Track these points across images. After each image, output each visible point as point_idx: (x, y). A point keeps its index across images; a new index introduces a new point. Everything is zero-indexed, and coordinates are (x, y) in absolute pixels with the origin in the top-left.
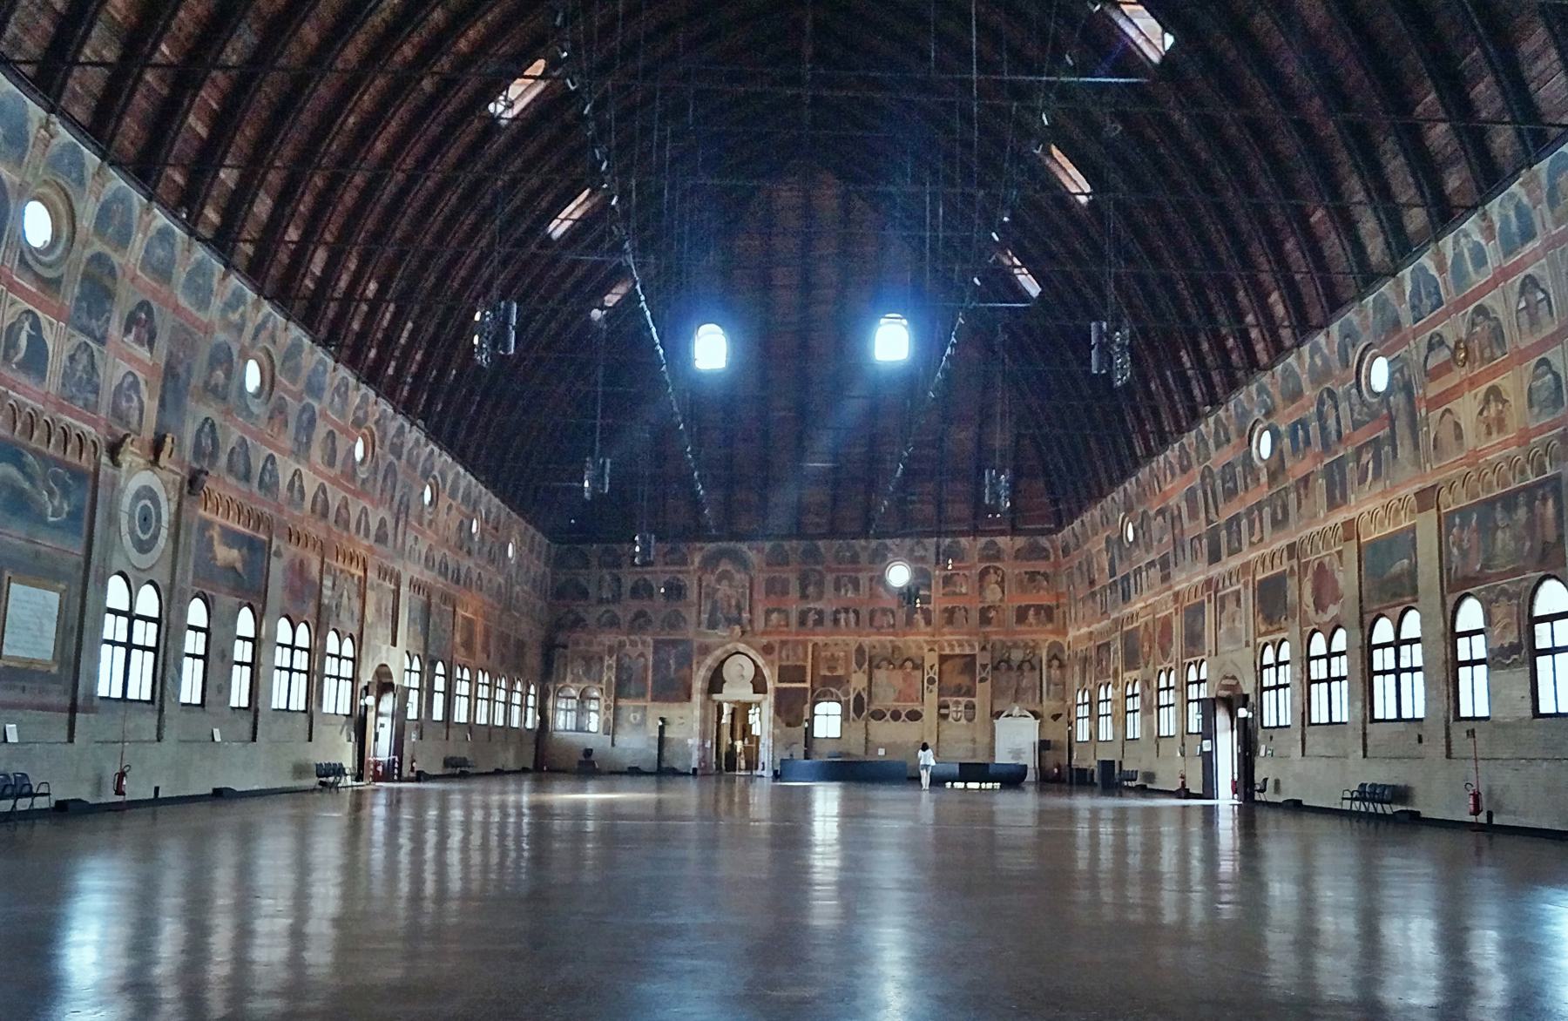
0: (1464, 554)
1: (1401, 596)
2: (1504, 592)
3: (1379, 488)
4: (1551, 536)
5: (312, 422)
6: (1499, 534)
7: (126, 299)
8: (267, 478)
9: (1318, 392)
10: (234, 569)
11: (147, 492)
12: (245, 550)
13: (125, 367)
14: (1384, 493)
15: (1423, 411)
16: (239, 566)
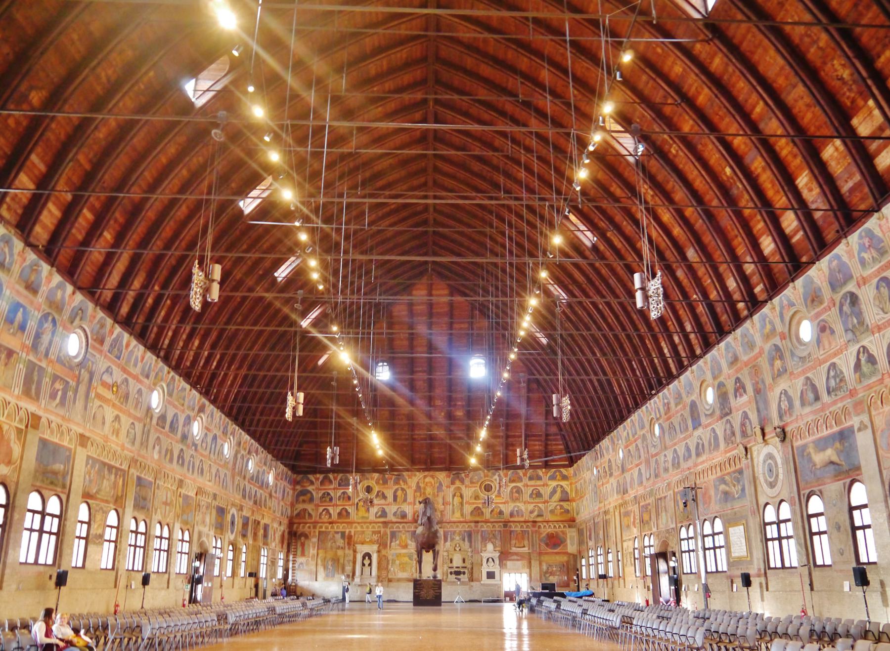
0: (90, 481)
1: (56, 485)
2: (101, 508)
3: (61, 412)
4: (120, 494)
5: (854, 299)
6: (105, 481)
7: (730, 387)
8: (832, 383)
9: (48, 310)
10: (832, 463)
11: (770, 456)
12: (838, 445)
13: (740, 412)
14: (63, 418)
15: (93, 395)
16: (835, 458)
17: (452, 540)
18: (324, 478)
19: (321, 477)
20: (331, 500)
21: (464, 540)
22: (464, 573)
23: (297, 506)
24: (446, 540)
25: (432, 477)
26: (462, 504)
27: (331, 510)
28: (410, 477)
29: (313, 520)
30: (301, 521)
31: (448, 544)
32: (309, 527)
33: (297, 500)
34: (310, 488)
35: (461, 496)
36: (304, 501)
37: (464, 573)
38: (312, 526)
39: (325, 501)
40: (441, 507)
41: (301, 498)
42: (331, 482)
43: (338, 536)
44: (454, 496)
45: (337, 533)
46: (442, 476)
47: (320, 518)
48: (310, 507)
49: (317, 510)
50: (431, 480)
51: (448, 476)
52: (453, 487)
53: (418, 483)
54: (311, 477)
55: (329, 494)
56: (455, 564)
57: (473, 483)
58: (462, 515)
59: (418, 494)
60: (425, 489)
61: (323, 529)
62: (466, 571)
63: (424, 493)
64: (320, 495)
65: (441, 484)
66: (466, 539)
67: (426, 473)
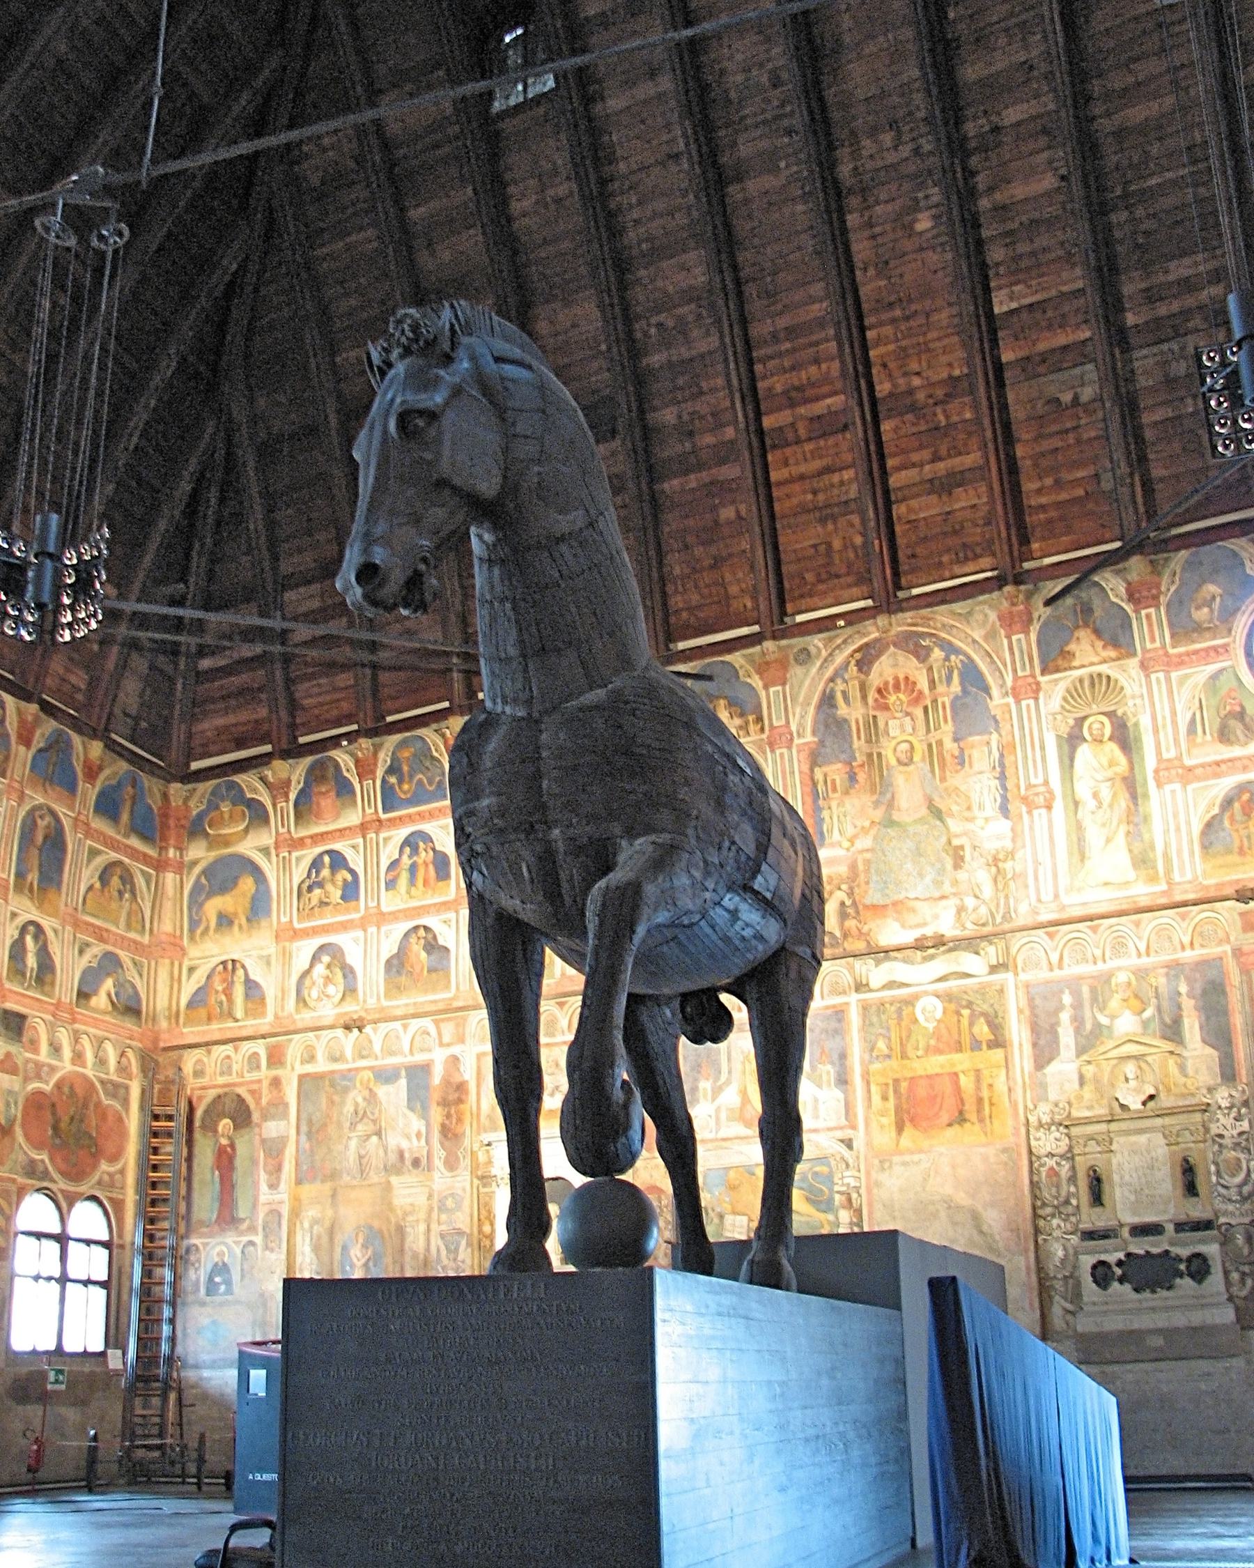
17: (1088, 1040)
18: (316, 775)
19: (296, 772)
20: (350, 891)
21: (1173, 1031)
22: (1199, 1268)
23: (194, 952)
24: (1044, 1053)
25: (915, 646)
26: (1131, 786)
27: (350, 944)
28: (774, 671)
29: (265, 1023)
30: (215, 1029)
31: (1064, 1068)
32: (254, 1058)
33: (194, 924)
34: (248, 847)
35: (1124, 736)
36: (225, 921)
37: (1199, 1268)
38: (260, 1047)
39: (323, 904)
40: (992, 832)
41: (213, 906)
42: (344, 790)
43: (394, 1095)
44: (1073, 740)
45: (386, 1076)
46: (977, 630)
47: (301, 1000)
48: (251, 949)
49: (286, 956)
50: (910, 666)
51: (1014, 622)
52: (1056, 688)
53: (828, 700)
54: (247, 781)
55: (338, 861)
56: (1124, 1208)
57: (1199, 629)
58: (1142, 861)
59: (836, 771)
60: (872, 730)
61: (322, 1065)
62: (1212, 1250)
63: (874, 760)
64: (299, 873)
65: (973, 679)
66: (1192, 1026)
67: (871, 631)
